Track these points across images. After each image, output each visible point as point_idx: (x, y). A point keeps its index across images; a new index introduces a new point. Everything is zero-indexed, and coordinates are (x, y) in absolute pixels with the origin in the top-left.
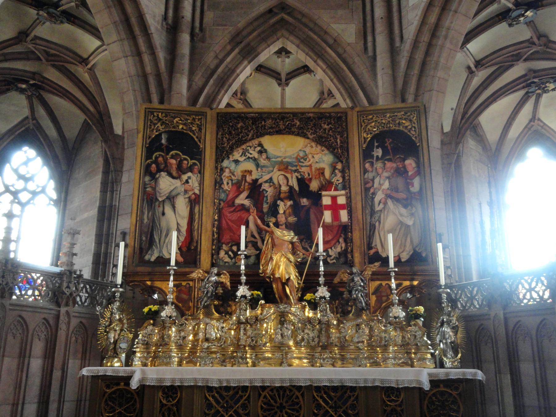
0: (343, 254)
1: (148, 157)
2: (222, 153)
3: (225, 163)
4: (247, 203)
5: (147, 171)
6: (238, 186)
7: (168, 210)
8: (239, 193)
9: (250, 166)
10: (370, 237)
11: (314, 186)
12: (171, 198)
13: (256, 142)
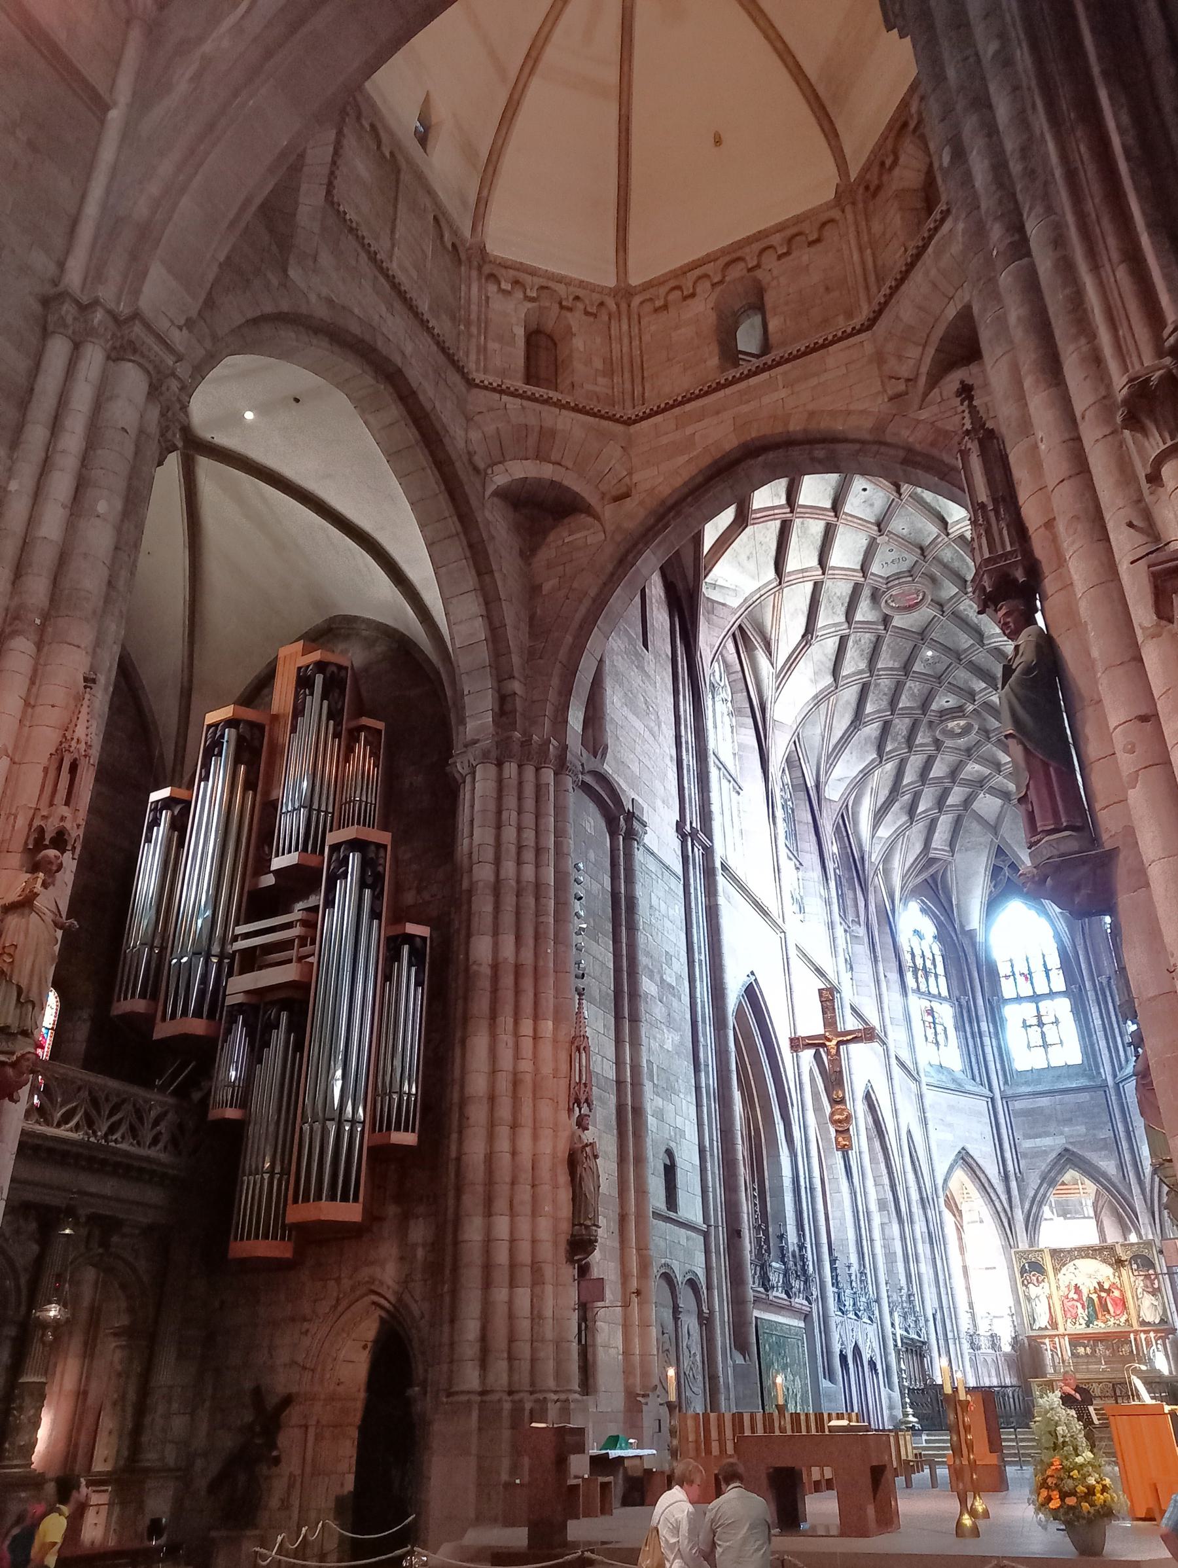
0: (1127, 1320)
11: (1106, 1286)
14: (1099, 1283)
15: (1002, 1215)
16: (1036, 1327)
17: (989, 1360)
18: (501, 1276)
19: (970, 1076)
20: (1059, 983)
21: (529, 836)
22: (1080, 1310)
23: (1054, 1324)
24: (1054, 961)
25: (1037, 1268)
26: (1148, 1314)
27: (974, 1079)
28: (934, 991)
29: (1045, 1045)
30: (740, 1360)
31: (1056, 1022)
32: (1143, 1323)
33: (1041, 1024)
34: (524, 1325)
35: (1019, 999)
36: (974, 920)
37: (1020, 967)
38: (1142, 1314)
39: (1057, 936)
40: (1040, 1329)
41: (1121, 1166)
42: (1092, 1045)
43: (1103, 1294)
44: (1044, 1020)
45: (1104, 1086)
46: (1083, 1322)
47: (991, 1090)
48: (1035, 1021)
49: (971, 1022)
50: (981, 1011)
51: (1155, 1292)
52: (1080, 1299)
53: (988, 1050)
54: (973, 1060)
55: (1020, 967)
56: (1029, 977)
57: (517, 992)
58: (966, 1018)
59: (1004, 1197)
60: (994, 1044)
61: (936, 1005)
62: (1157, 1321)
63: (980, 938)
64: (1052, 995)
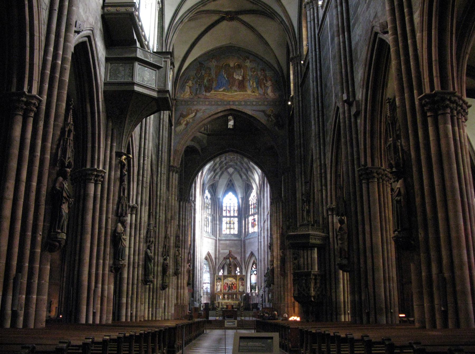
18: (180, 288)
20: (236, 215)
21: (184, 216)
23: (221, 290)
24: (236, 208)
29: (230, 228)
31: (234, 223)
32: (239, 291)
33: (230, 223)
34: (182, 295)
35: (226, 217)
36: (220, 196)
37: (228, 208)
39: (238, 203)
41: (241, 258)
44: (232, 222)
45: (241, 240)
51: (243, 285)
55: (228, 208)
56: (230, 212)
58: (214, 219)
63: (221, 200)
64: (234, 217)
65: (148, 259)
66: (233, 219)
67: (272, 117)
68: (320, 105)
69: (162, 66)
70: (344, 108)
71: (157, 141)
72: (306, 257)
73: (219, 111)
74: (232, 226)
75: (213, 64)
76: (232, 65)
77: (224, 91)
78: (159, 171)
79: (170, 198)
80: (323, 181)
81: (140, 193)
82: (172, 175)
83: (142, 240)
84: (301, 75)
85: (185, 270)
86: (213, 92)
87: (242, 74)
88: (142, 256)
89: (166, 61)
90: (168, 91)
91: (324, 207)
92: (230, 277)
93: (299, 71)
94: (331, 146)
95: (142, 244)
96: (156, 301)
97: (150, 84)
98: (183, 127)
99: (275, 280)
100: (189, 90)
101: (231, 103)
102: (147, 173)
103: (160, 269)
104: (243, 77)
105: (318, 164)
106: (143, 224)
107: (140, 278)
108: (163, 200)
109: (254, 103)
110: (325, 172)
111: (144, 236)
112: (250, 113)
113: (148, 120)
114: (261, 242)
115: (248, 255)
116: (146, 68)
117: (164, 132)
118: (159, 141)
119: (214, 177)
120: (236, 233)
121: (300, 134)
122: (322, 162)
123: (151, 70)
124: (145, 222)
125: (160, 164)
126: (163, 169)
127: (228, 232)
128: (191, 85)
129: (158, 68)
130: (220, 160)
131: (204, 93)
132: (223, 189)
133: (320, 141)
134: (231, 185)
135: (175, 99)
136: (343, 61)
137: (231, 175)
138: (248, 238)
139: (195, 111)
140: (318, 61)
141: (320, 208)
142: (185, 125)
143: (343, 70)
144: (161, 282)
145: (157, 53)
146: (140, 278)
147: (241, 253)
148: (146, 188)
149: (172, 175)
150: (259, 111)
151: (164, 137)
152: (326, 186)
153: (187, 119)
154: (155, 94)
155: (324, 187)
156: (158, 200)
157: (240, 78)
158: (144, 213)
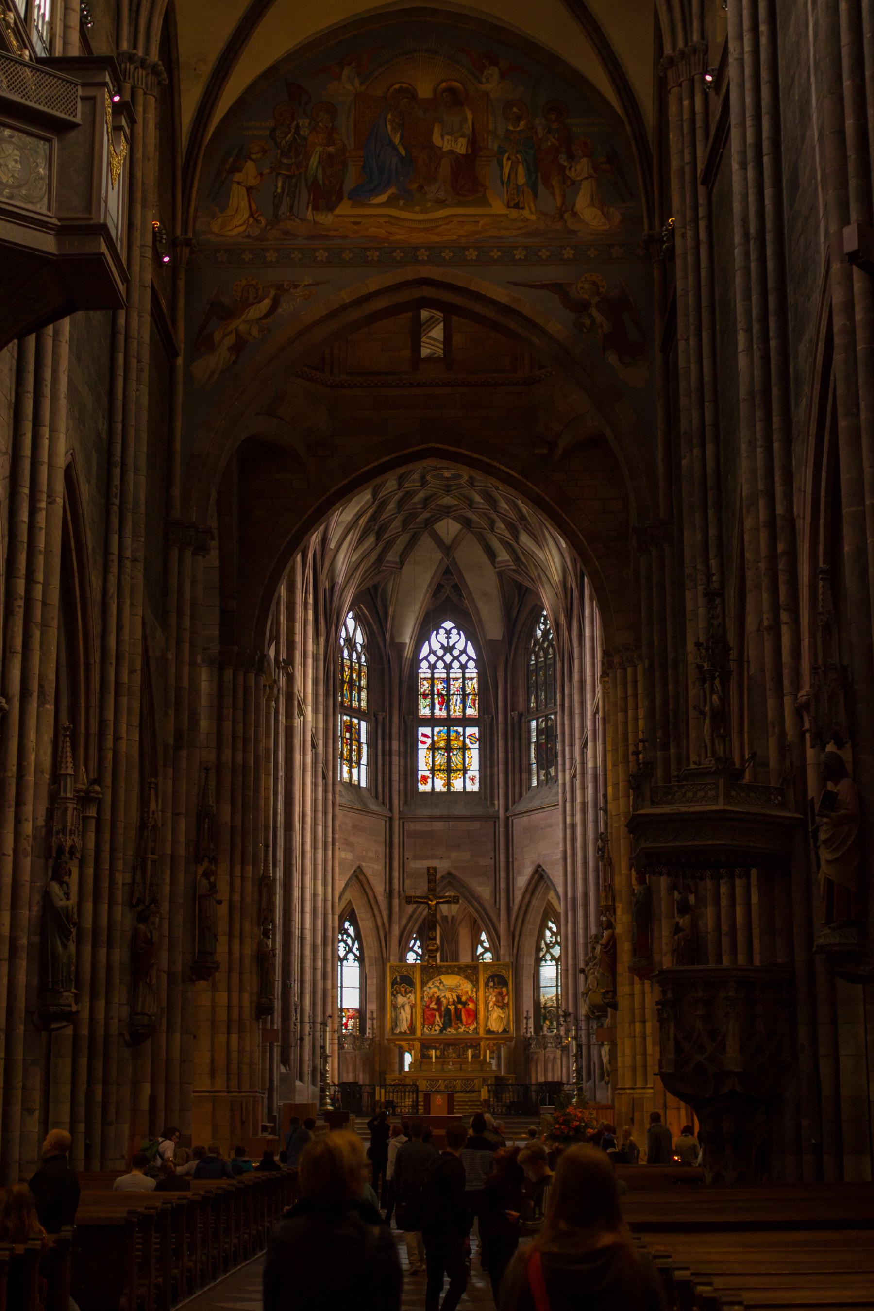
0: (476, 1029)
1: (392, 987)
2: (423, 984)
3: (425, 988)
4: (435, 1007)
5: (392, 994)
6: (431, 998)
7: (402, 1011)
8: (431, 1002)
9: (436, 990)
10: (487, 1022)
11: (464, 999)
12: (403, 1006)
13: (438, 978)
14: (459, 997)
15: (381, 929)
16: (397, 1031)
17: (349, 1057)
19: (374, 795)
21: (240, 727)
22: (437, 1016)
23: (412, 1028)
25: (407, 981)
26: (494, 1025)
27: (377, 797)
28: (355, 704)
29: (449, 770)
30: (283, 1070)
31: (464, 748)
32: (489, 1032)
33: (448, 749)
35: (432, 722)
38: (489, 1024)
40: (400, 1032)
41: (495, 893)
42: (492, 776)
43: (460, 1006)
45: (495, 818)
46: (437, 1028)
47: (391, 810)
48: (442, 744)
49: (383, 739)
50: (395, 731)
51: (503, 1007)
52: (439, 1010)
53: (395, 769)
54: (380, 778)
56: (446, 701)
57: (233, 845)
59: (385, 914)
60: (402, 763)
61: (355, 721)
62: (500, 1031)
63: (408, 653)
64: (465, 722)
65: (53, 922)
66: (460, 729)
67: (594, 312)
68: (770, 265)
69: (78, 120)
70: (851, 288)
71: (102, 426)
72: (724, 902)
73: (372, 289)
74: (456, 760)
75: (345, 87)
76: (425, 91)
77: (391, 202)
78: (115, 549)
79: (171, 656)
80: (783, 590)
81: (19, 648)
82: (181, 561)
83: (27, 845)
84: (707, 128)
85: (248, 950)
86: (345, 208)
87: (468, 129)
88: (28, 913)
89: (93, 98)
90: (103, 229)
91: (787, 700)
92: (450, 971)
93: (699, 118)
94: (812, 440)
95: (27, 862)
96: (104, 1095)
97: (27, 199)
98: (221, 357)
99: (620, 989)
100: (244, 204)
101: (423, 255)
102: (47, 563)
103: (120, 955)
104: (473, 142)
105: (762, 517)
106: (30, 778)
107: (21, 1004)
108: (132, 672)
109: (520, 254)
110: (792, 554)
111: (35, 828)
112: (499, 294)
113: (49, 343)
114: (573, 826)
115: (521, 882)
116: (7, 132)
117: (133, 384)
118: (111, 421)
119: (380, 560)
120: (474, 787)
121: (701, 390)
122: (780, 510)
123: (29, 139)
124: (38, 770)
125: (115, 520)
126: (128, 541)
127: (440, 785)
128: (252, 182)
129: (58, 127)
130: (400, 486)
131: (309, 214)
132: (417, 607)
133: (768, 419)
134: (448, 590)
135: (188, 243)
136: (847, 83)
137: (447, 549)
138: (521, 807)
139: (273, 292)
140: (765, 75)
141: (771, 703)
142: (231, 349)
143: (849, 123)
144: (125, 1010)
145: (50, 62)
146: (21, 1004)
147: (496, 870)
148: (44, 626)
149: (181, 561)
150: (544, 287)
151: (133, 407)
152: (794, 610)
153: (239, 324)
154: (47, 243)
155: (784, 616)
156: (112, 671)
157: (461, 147)
158: (38, 732)
